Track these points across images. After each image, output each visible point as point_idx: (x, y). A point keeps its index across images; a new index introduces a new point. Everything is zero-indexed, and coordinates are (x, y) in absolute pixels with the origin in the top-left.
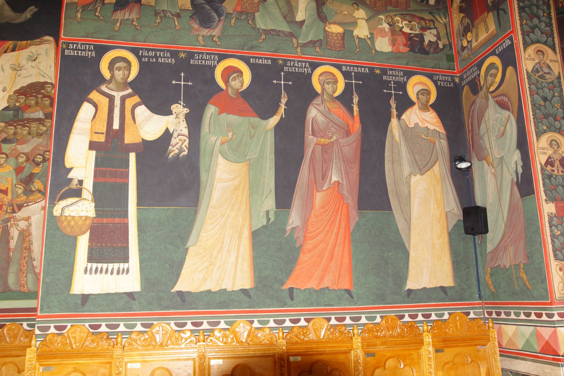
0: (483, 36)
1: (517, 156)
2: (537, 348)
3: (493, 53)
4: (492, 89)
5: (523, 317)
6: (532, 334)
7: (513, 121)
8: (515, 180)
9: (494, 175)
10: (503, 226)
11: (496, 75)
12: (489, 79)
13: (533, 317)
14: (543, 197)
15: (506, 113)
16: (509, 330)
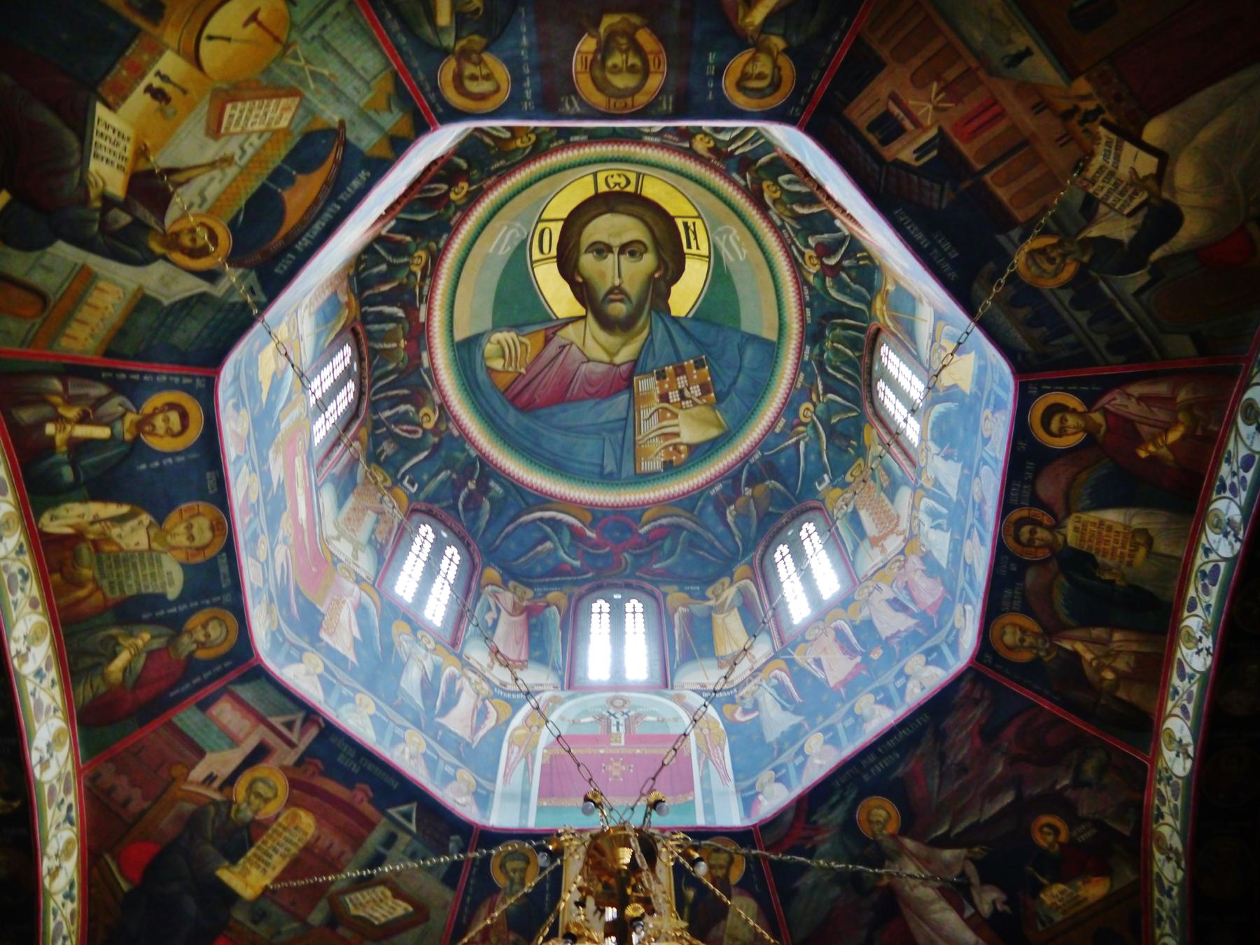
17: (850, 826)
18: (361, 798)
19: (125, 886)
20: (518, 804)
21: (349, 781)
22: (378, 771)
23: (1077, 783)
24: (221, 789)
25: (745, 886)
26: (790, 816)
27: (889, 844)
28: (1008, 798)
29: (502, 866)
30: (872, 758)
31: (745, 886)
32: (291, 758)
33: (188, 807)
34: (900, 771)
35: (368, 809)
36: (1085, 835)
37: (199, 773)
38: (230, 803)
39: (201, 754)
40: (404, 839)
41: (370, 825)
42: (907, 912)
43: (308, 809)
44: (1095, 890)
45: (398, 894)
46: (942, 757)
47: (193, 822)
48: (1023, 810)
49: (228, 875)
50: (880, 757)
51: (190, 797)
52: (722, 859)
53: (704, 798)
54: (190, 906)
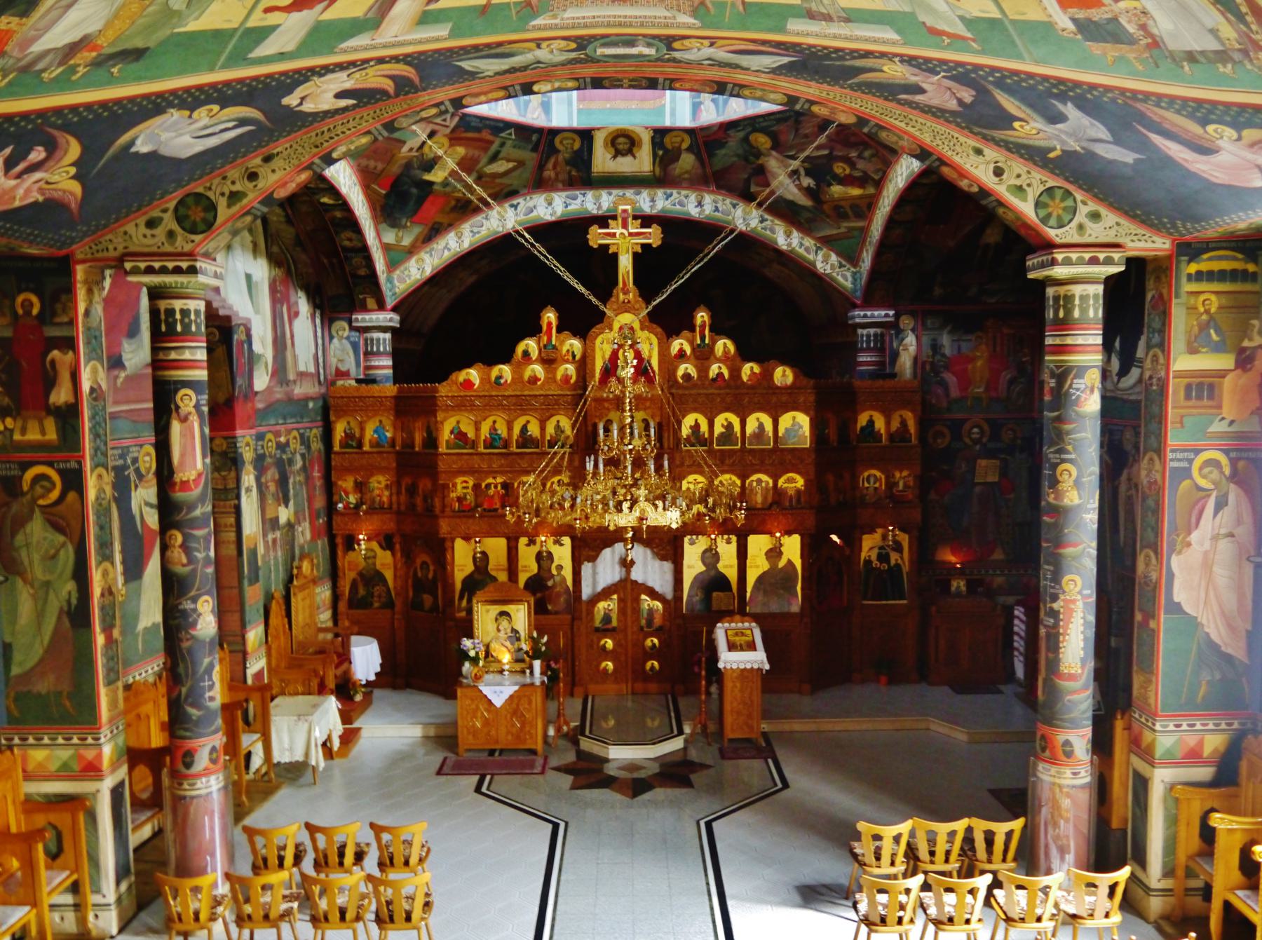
0: (33, 435)
1: (71, 586)
2: (76, 767)
3: (50, 464)
4: (41, 502)
5: (60, 741)
6: (72, 757)
7: (70, 549)
8: (66, 608)
9: (34, 597)
10: (41, 652)
11: (50, 490)
12: (39, 490)
13: (75, 741)
14: (98, 629)
15: (61, 538)
16: (38, 755)
17: (746, 139)
18: (486, 135)
19: (384, 192)
20: (566, 106)
21: (478, 130)
22: (492, 123)
23: (860, 156)
24: (417, 151)
25: (689, 150)
26: (715, 129)
27: (764, 151)
28: (826, 152)
29: (561, 142)
30: (761, 120)
31: (689, 150)
32: (448, 131)
33: (404, 161)
34: (774, 128)
35: (490, 138)
36: (857, 174)
37: (405, 149)
38: (423, 155)
39: (404, 143)
40: (509, 143)
41: (492, 143)
42: (768, 174)
43: (460, 145)
44: (856, 192)
45: (508, 161)
46: (797, 130)
47: (408, 165)
48: (831, 158)
49: (428, 177)
50: (765, 121)
51: (403, 158)
52: (678, 139)
53: (671, 102)
54: (414, 191)
